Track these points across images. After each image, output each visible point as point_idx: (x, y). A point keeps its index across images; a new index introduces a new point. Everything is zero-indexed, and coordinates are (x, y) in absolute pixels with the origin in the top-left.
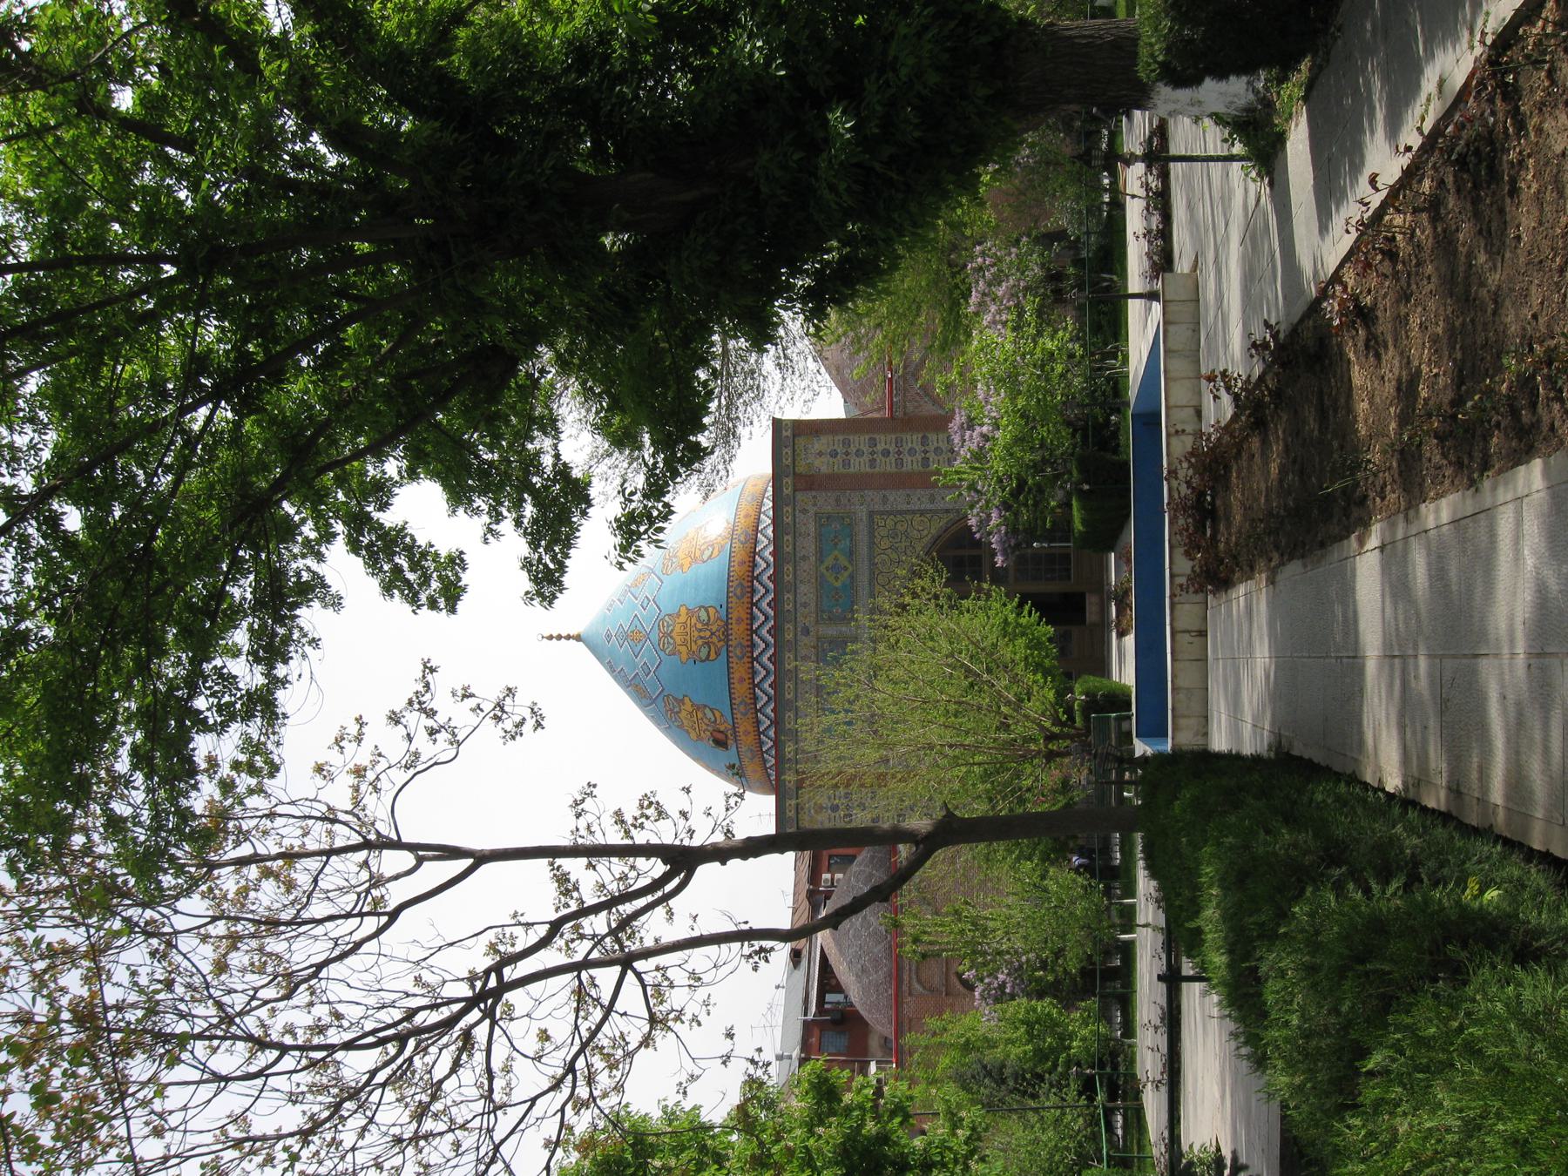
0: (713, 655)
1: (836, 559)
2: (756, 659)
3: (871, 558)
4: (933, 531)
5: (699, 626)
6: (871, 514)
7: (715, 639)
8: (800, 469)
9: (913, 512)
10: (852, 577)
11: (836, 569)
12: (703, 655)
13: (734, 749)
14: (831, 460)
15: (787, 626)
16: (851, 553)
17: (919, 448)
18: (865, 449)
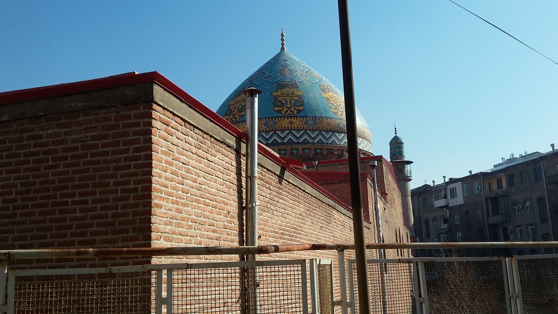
0: (276, 109)
2: (275, 133)
5: (293, 101)
7: (286, 109)
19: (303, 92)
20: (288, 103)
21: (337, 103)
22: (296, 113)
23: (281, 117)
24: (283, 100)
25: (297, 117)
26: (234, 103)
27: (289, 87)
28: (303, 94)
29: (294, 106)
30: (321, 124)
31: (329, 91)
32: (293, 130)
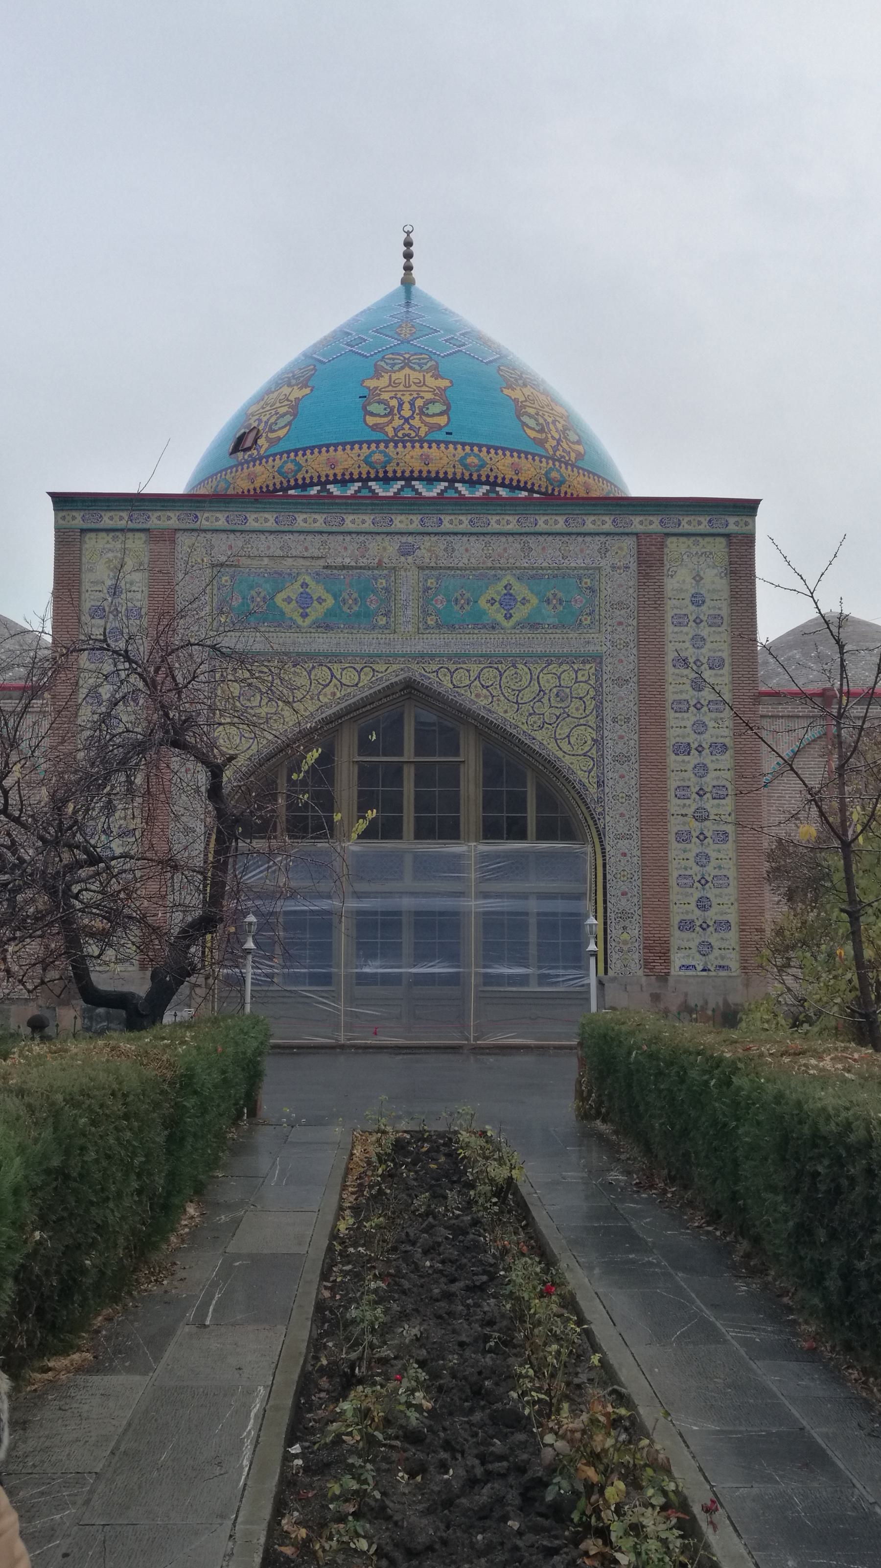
0: (371, 420)
1: (524, 601)
3: (527, 658)
4: (567, 760)
5: (419, 403)
6: (597, 659)
8: (672, 544)
9: (599, 728)
10: (494, 626)
11: (508, 601)
12: (371, 408)
13: (232, 462)
14: (688, 596)
15: (416, 519)
16: (534, 626)
17: (707, 738)
18: (705, 652)
19: (451, 382)
20: (406, 406)
21: (546, 417)
22: (426, 435)
23: (387, 443)
24: (391, 398)
25: (430, 443)
26: (261, 411)
27: (411, 368)
28: (446, 388)
29: (422, 413)
30: (494, 467)
31: (525, 385)
32: (416, 479)
